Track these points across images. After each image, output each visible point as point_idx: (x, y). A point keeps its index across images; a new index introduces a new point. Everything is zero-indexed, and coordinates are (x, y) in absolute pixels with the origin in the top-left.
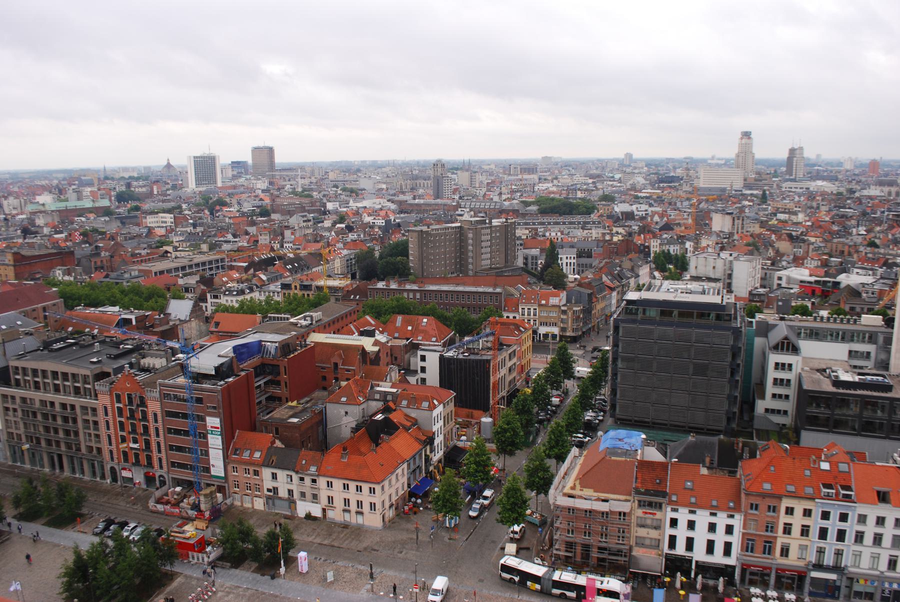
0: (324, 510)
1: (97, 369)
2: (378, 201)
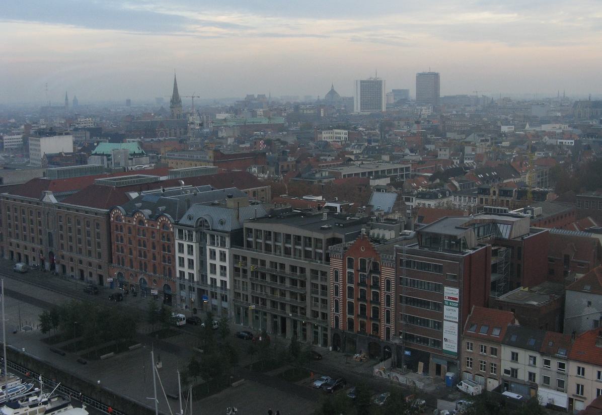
0: (571, 401)
1: (329, 235)
2: (557, 126)
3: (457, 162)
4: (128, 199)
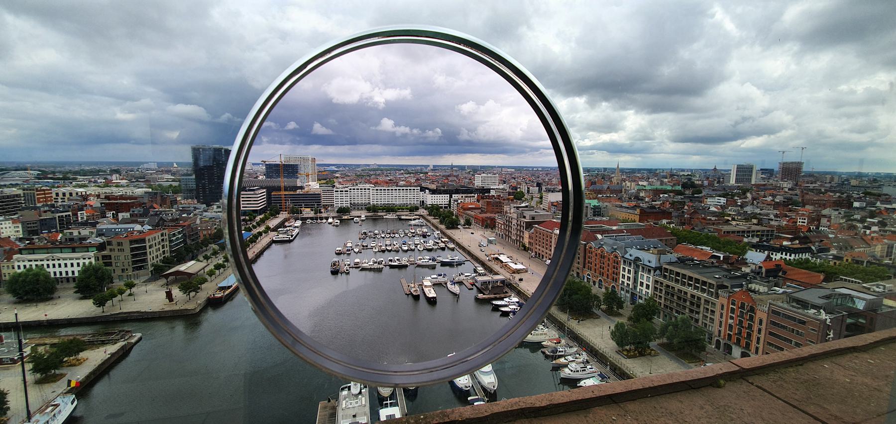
3: (813, 228)
4: (596, 239)
